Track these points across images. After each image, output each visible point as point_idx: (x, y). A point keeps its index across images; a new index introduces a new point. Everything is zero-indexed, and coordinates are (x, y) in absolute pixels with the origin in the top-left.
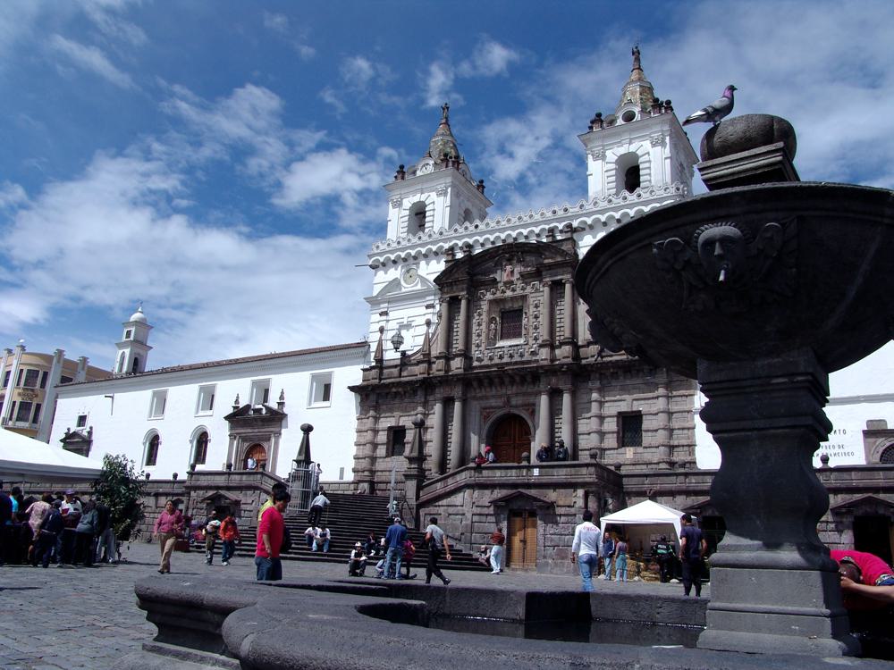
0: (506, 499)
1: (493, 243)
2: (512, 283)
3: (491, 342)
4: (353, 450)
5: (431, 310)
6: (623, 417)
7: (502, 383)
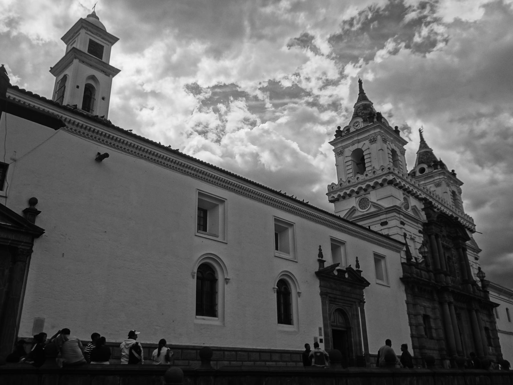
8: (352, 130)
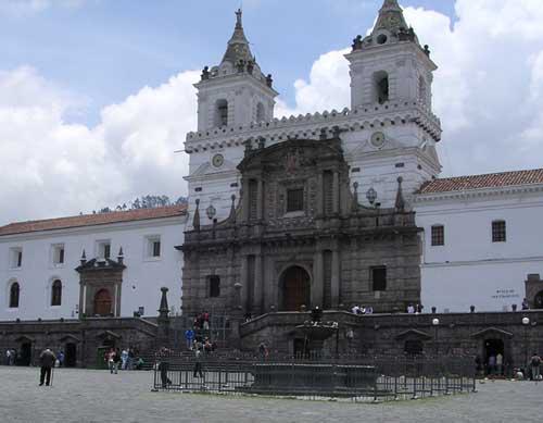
0: (292, 334)
1: (280, 138)
2: (295, 169)
3: (281, 212)
4: (181, 293)
5: (234, 188)
7: (289, 245)
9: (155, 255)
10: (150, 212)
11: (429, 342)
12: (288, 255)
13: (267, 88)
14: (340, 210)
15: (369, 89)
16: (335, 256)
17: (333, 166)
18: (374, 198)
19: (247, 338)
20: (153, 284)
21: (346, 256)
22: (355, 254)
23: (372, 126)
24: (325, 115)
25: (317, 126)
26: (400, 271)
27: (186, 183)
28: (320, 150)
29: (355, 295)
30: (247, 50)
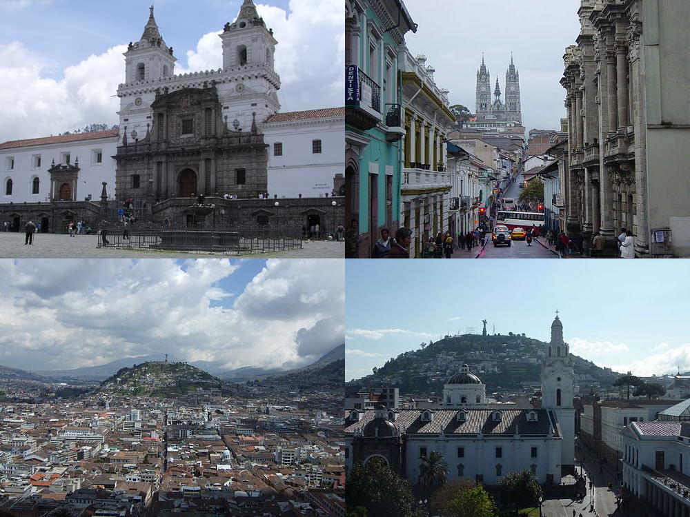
0: (185, 212)
1: (178, 88)
2: (187, 107)
3: (178, 134)
4: (115, 186)
5: (149, 119)
6: (238, 172)
8: (140, 47)
9: (98, 162)
10: (96, 134)
11: (273, 217)
12: (183, 161)
13: (169, 56)
14: (216, 134)
15: (235, 56)
16: (213, 162)
17: (211, 105)
18: (237, 125)
19: (157, 214)
20: (97, 180)
21: (220, 162)
22: (225, 161)
23: (236, 80)
24: (207, 73)
25: (201, 80)
26: (254, 172)
27: (118, 116)
28: (204, 95)
29: (225, 187)
30: (157, 32)
